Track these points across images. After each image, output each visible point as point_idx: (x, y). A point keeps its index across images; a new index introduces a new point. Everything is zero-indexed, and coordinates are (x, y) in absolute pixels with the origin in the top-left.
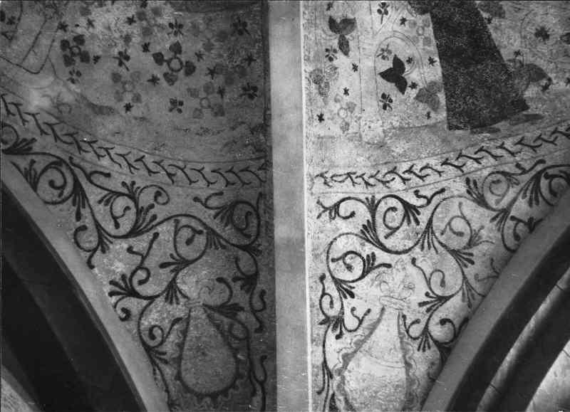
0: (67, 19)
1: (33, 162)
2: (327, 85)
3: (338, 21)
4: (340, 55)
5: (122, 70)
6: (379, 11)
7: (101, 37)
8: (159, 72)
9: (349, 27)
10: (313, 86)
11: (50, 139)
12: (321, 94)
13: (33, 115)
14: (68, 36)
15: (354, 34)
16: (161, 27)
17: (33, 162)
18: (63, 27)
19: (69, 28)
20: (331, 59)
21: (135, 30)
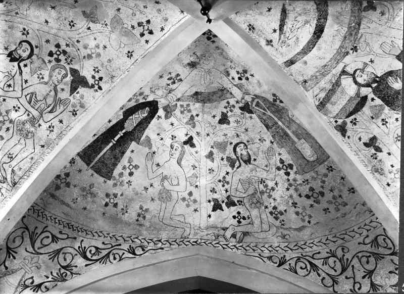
0: (266, 204)
1: (290, 264)
2: (382, 169)
3: (368, 142)
4: (379, 154)
5: (297, 209)
6: (383, 124)
7: (281, 202)
8: (311, 202)
9: (374, 141)
10: (376, 174)
11: (290, 251)
12: (382, 175)
13: (278, 247)
14: (270, 209)
15: (378, 141)
16: (300, 185)
17: (290, 264)
18: (266, 207)
19: (269, 206)
20: (376, 158)
21: (292, 191)
